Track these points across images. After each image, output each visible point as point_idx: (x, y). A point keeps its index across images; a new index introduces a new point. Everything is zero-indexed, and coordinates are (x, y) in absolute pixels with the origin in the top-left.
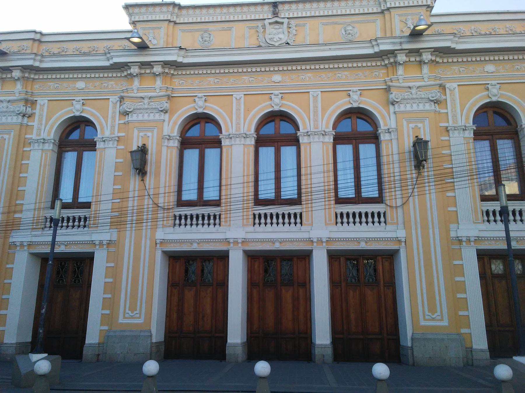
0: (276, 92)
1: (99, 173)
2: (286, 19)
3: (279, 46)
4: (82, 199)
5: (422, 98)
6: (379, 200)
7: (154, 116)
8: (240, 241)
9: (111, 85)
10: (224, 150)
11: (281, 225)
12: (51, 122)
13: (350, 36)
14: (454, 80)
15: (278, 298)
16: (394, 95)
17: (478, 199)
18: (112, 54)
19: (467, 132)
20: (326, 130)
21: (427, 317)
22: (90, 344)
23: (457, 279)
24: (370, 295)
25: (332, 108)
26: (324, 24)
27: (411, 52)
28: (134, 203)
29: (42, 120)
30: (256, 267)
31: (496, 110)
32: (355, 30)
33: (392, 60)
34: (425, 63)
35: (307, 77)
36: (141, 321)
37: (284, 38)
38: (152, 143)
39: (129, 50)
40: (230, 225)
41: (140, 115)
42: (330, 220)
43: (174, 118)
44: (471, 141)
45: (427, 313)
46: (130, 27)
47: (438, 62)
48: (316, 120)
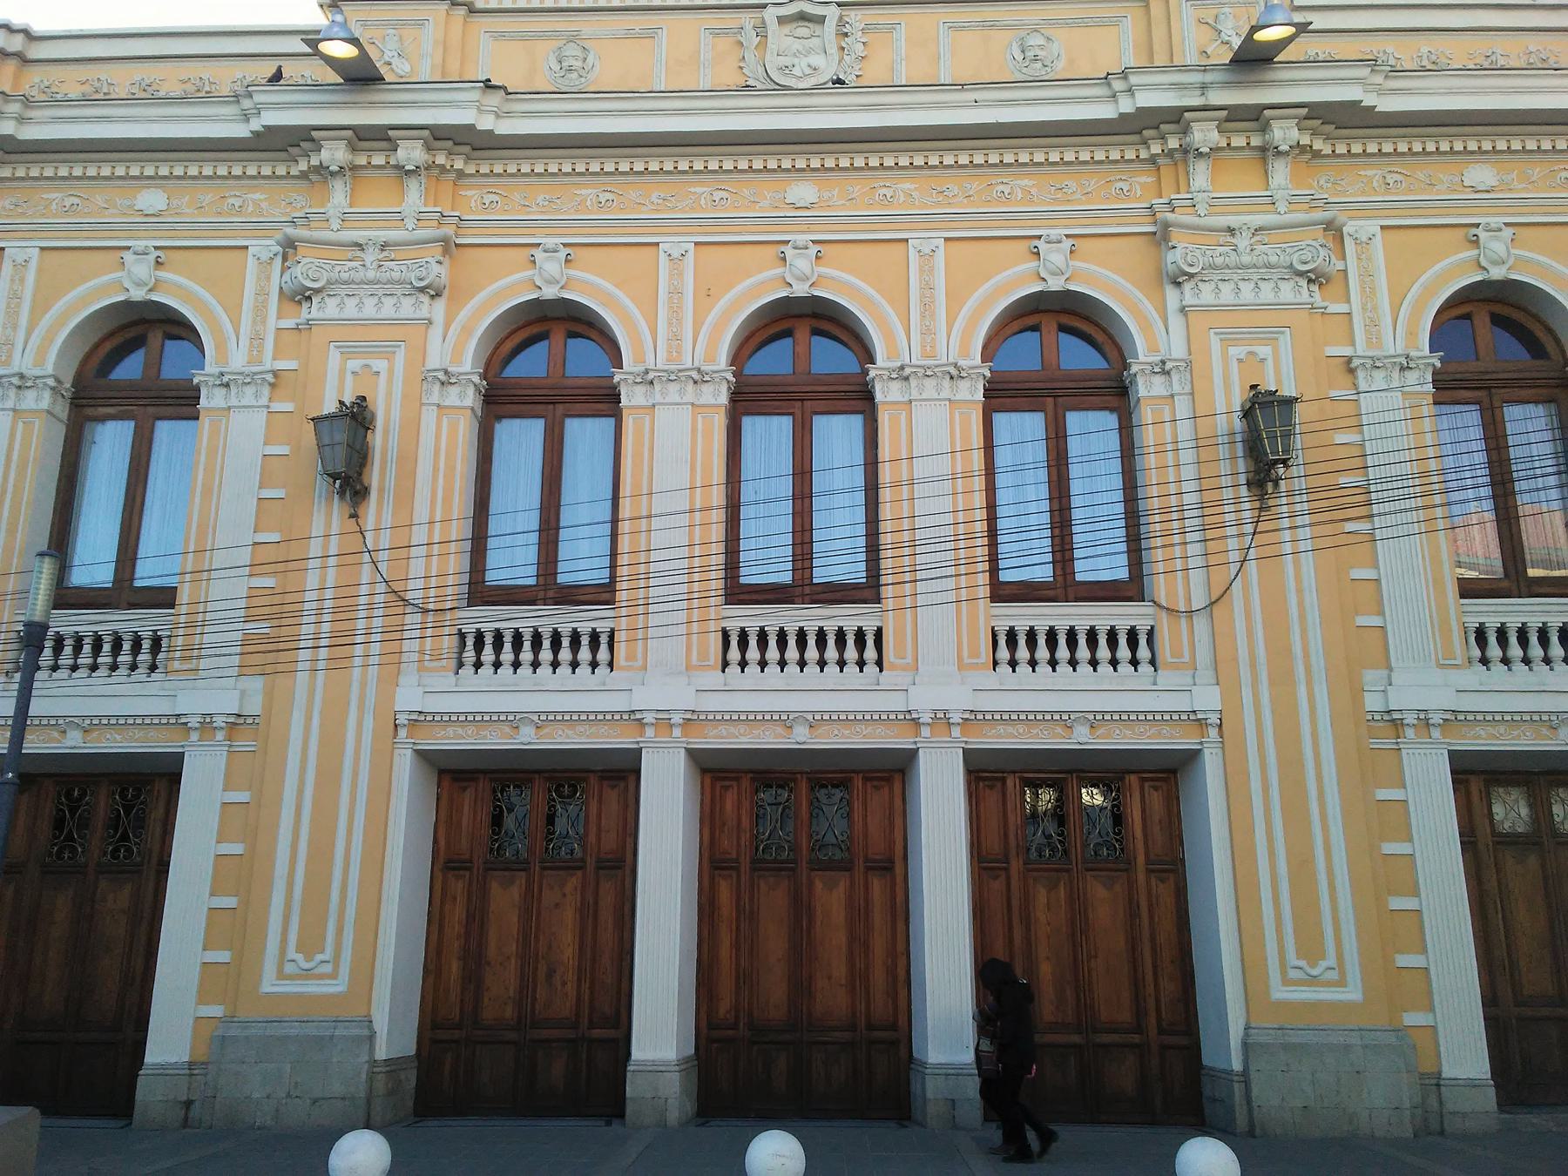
0: (802, 239)
1: (207, 491)
2: (834, 8)
4: (147, 573)
5: (1269, 266)
6: (1131, 589)
7: (397, 306)
8: (677, 718)
9: (256, 203)
10: (629, 422)
11: (812, 669)
12: (47, 320)
13: (1039, 65)
14: (1364, 210)
15: (801, 911)
16: (1181, 254)
17: (1452, 590)
18: (258, 98)
20: (961, 363)
21: (1293, 974)
22: (162, 1066)
23: (1389, 848)
24: (1103, 898)
25: (980, 293)
26: (955, 27)
29: (17, 313)
30: (729, 806)
31: (1498, 309)
32: (1055, 48)
33: (1173, 143)
34: (1279, 154)
35: (904, 191)
36: (338, 986)
38: (389, 394)
39: (316, 86)
42: (974, 653)
43: (463, 315)
45: (1292, 959)
47: (1317, 154)
48: (930, 324)
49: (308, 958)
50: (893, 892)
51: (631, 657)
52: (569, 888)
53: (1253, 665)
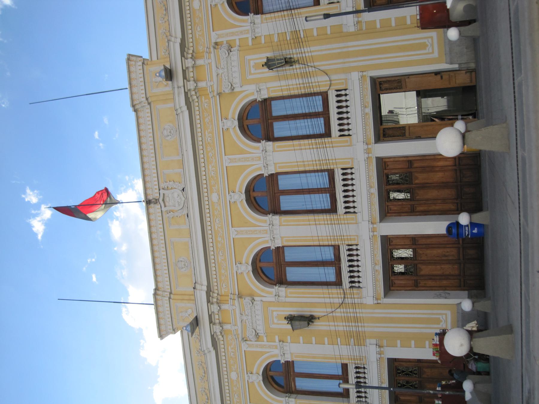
0: (228, 198)
2: (160, 191)
3: (186, 198)
6: (325, 96)
8: (371, 226)
9: (232, 349)
13: (172, 131)
18: (205, 349)
19: (256, 21)
20: (261, 149)
21: (431, 51)
25: (238, 142)
27: (185, 77)
28: (340, 326)
30: (395, 208)
33: (193, 93)
36: (449, 313)
37: (177, 192)
38: (283, 311)
40: (357, 236)
41: (258, 322)
42: (347, 141)
44: (264, 16)
46: (179, 333)
49: (441, 321)
50: (417, 160)
51: (354, 239)
52: (421, 252)
53: (344, 63)
